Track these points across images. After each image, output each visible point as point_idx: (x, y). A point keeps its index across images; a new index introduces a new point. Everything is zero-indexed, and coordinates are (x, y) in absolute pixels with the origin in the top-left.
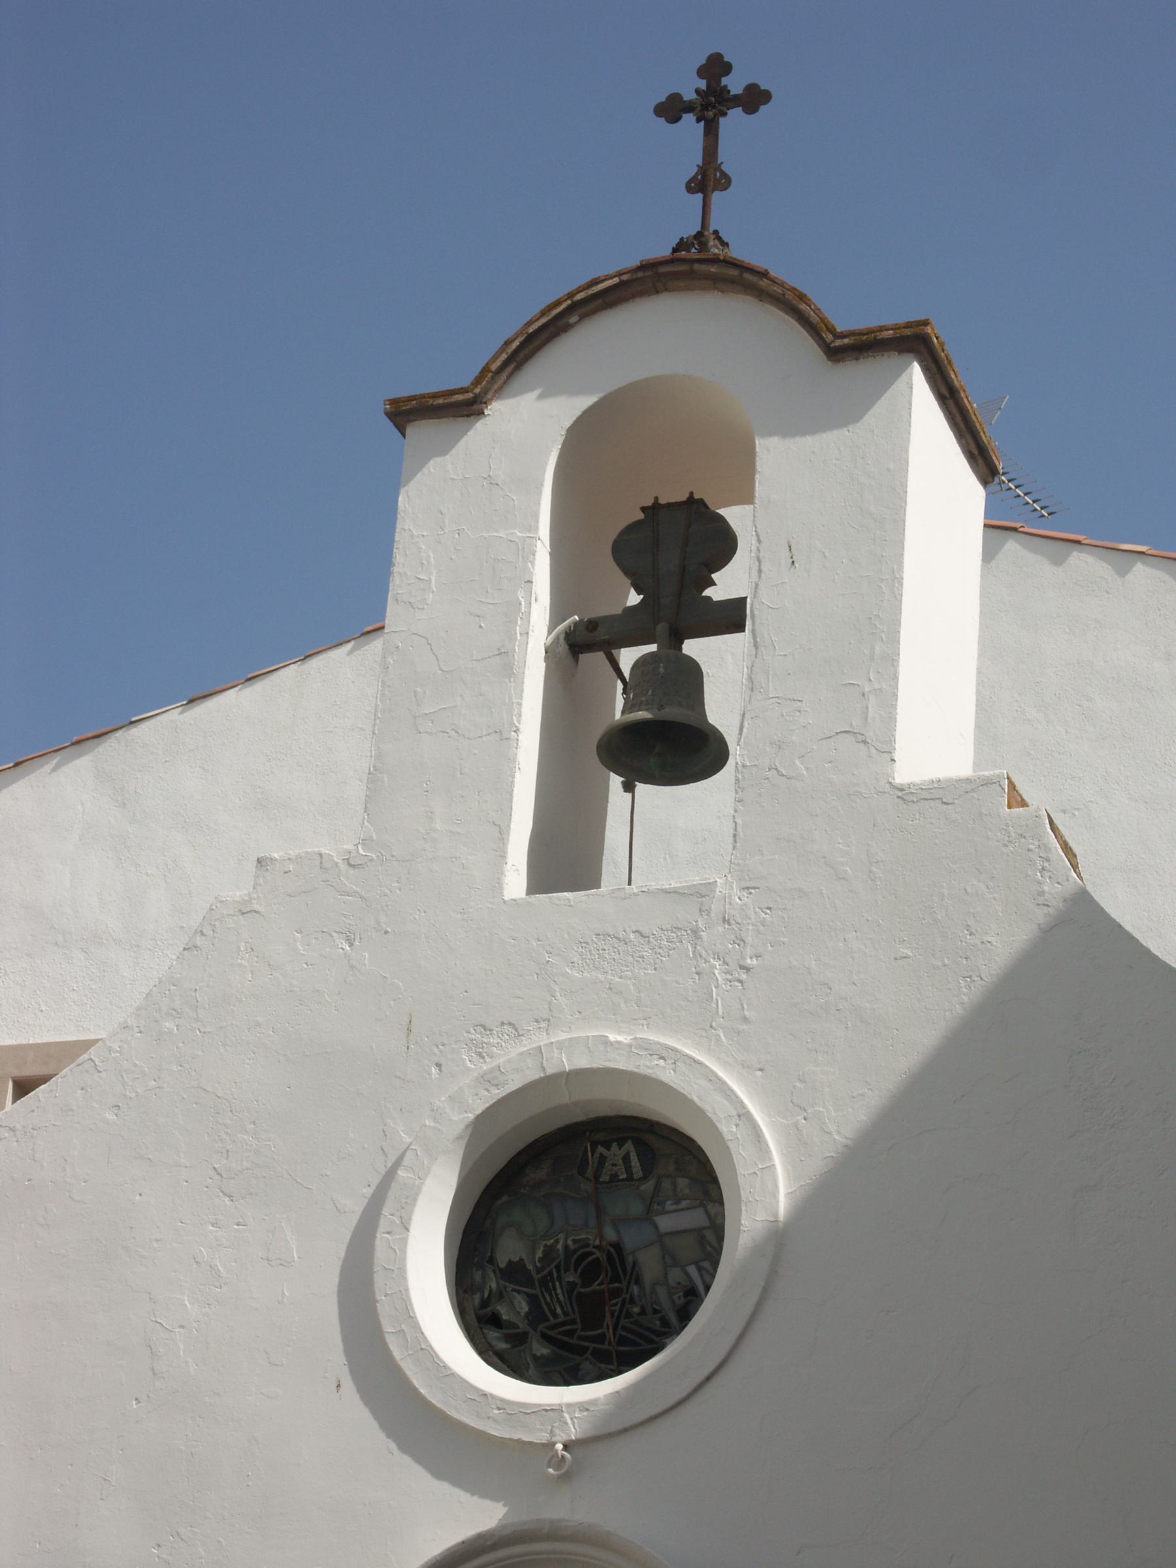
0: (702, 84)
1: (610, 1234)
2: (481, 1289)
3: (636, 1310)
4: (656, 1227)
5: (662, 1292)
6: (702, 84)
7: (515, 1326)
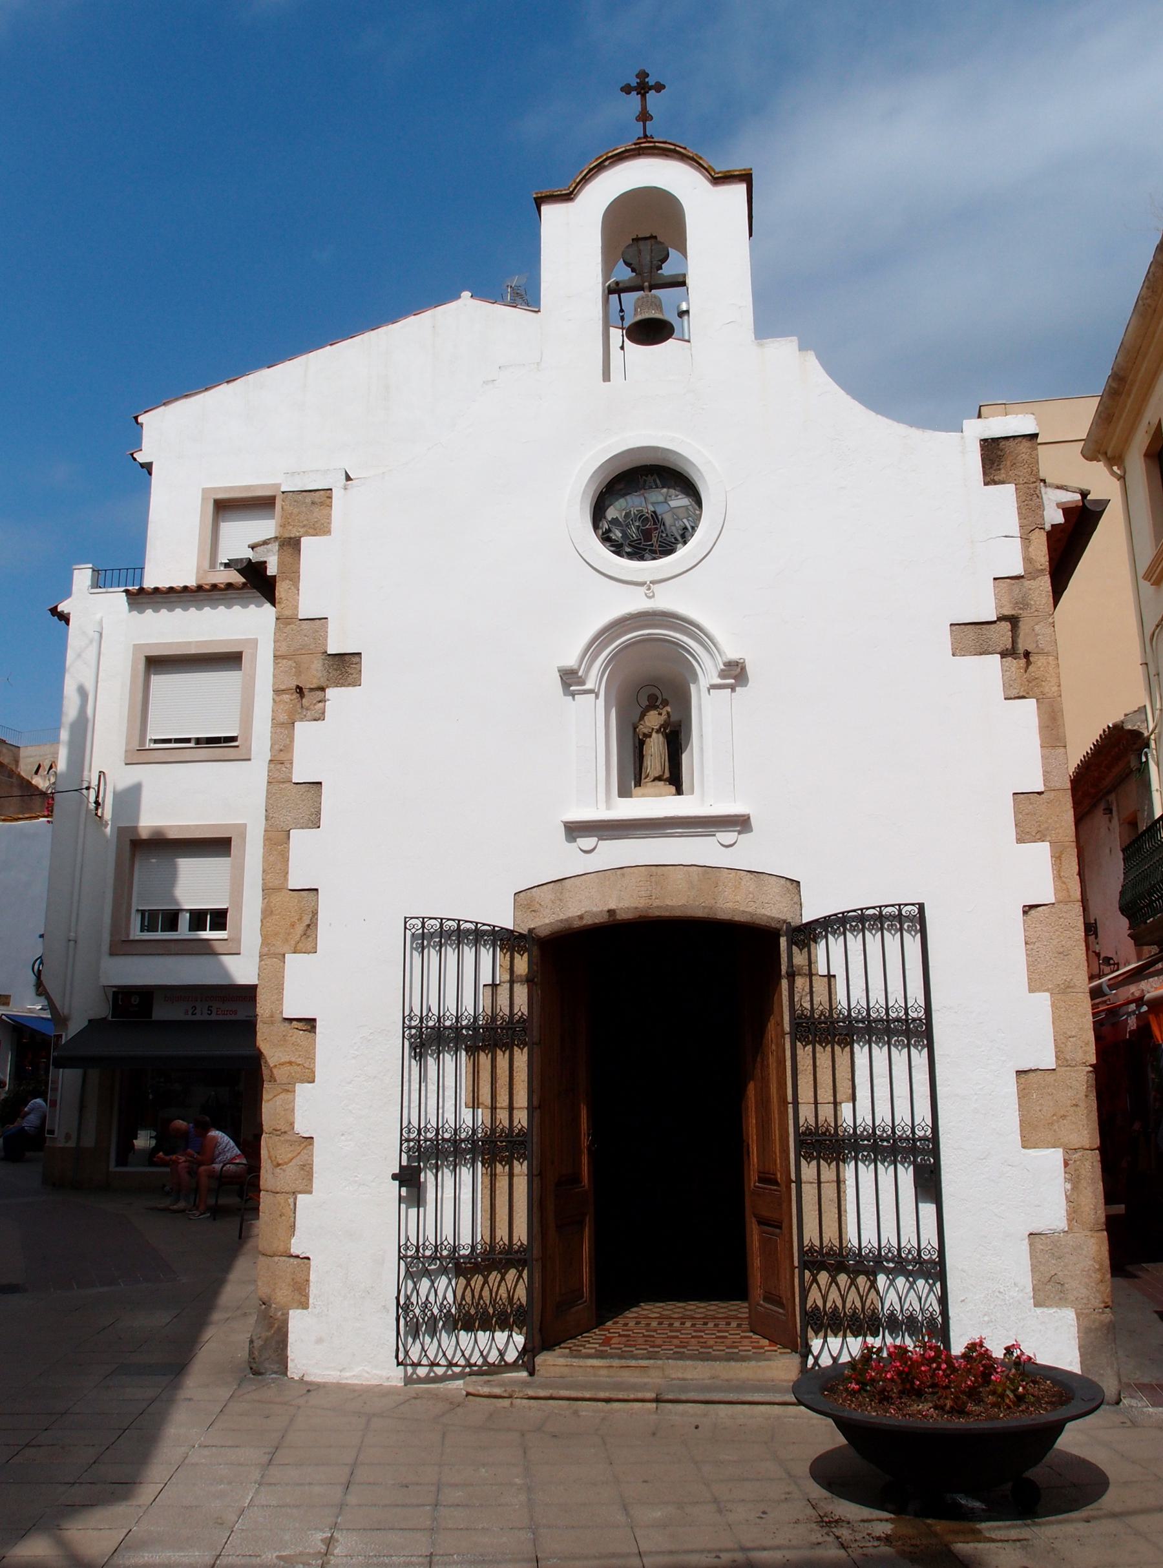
1: (651, 508)
2: (602, 528)
3: (664, 535)
5: (673, 528)
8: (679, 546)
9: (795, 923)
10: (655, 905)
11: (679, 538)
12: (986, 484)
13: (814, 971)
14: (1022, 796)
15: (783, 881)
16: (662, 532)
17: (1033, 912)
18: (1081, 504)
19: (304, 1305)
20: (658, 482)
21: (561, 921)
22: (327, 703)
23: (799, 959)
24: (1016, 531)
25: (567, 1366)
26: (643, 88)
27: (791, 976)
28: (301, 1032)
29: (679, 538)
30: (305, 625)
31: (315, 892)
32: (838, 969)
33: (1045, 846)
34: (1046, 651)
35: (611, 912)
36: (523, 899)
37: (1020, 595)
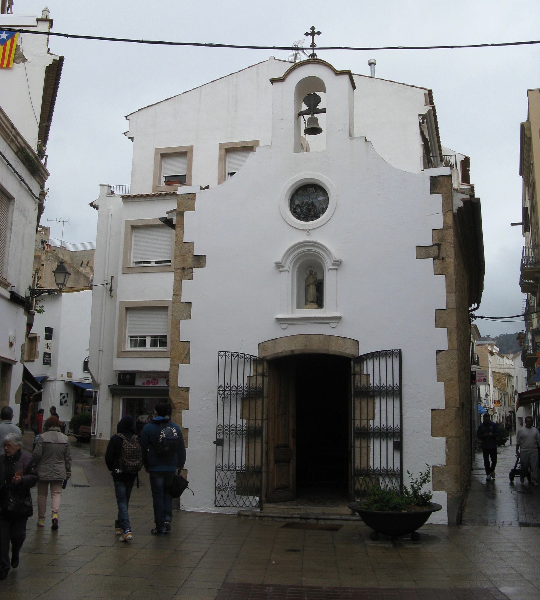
0: (311, 31)
1: (311, 200)
3: (316, 211)
4: (318, 199)
5: (319, 208)
6: (311, 31)
7: (299, 213)
8: (321, 215)
9: (356, 356)
10: (307, 349)
11: (321, 212)
12: (431, 194)
13: (362, 373)
14: (439, 311)
15: (353, 341)
16: (315, 209)
18: (470, 199)
23: (357, 369)
24: (441, 212)
25: (273, 508)
26: (313, 34)
27: (355, 374)
28: (184, 392)
29: (321, 212)
30: (186, 245)
32: (370, 372)
33: (446, 328)
35: (292, 351)
36: (262, 346)
37: (442, 236)
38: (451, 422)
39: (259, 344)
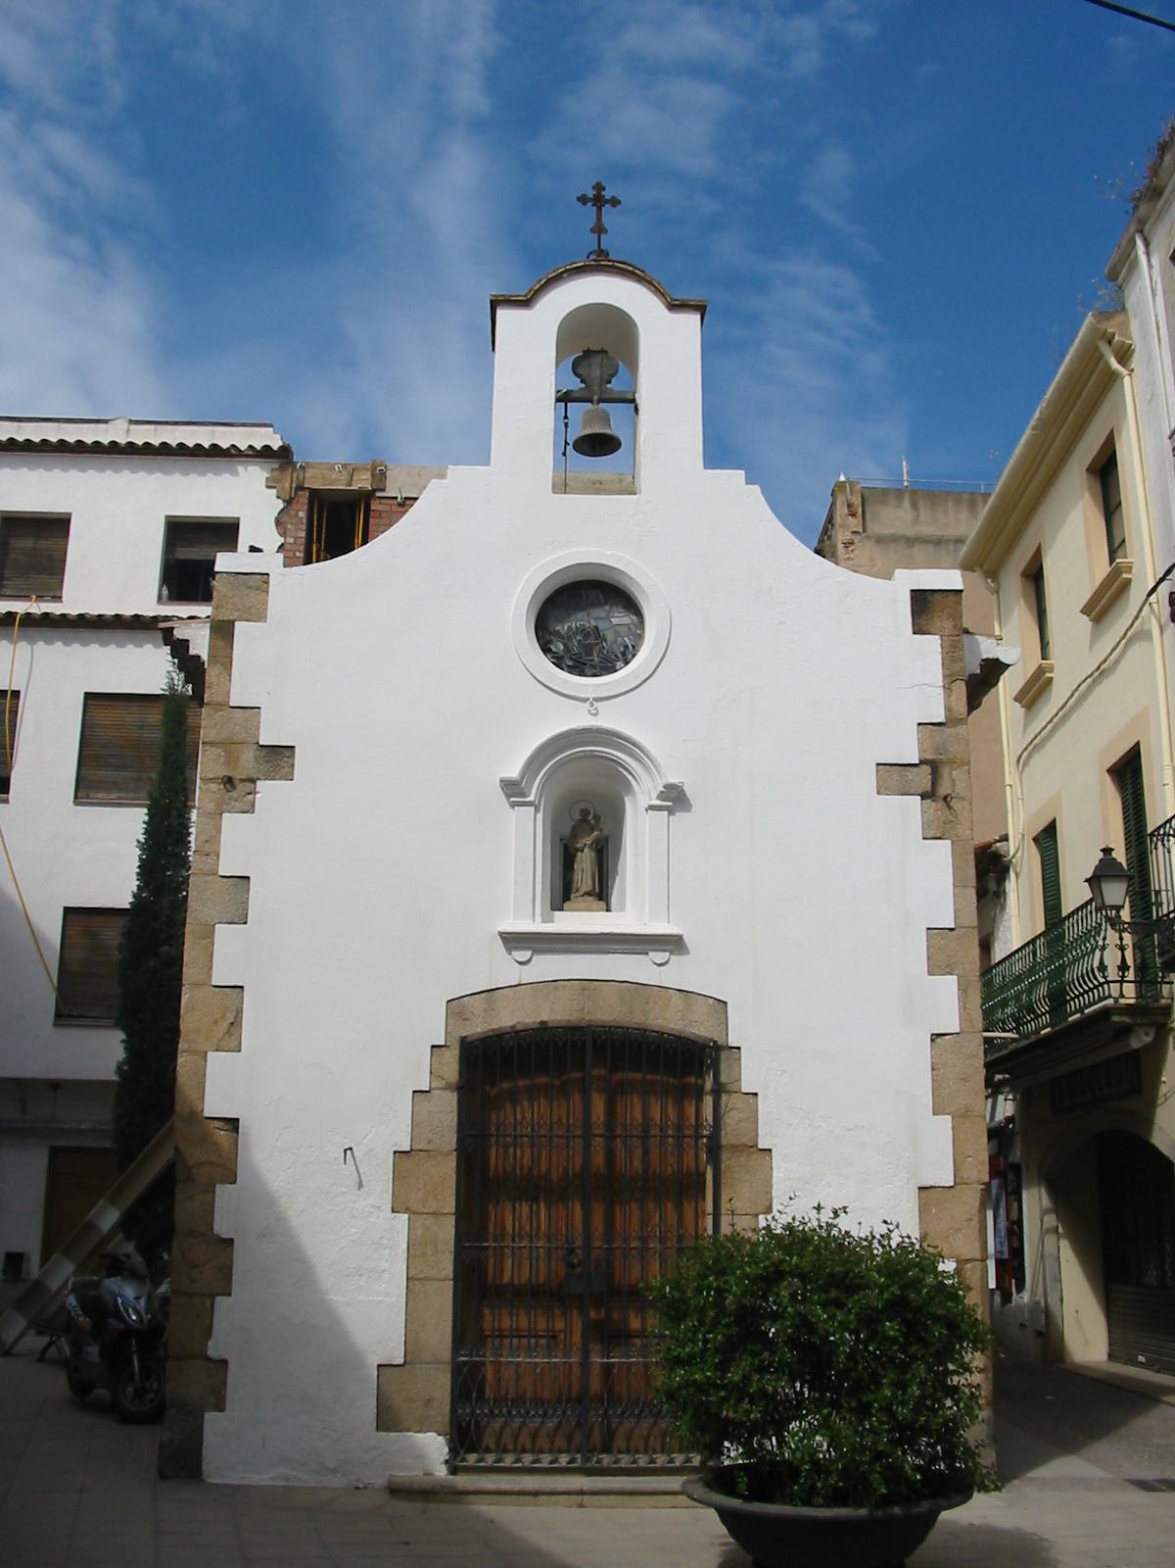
1: (593, 623)
11: (619, 655)
17: (939, 1040)
19: (220, 1407)
20: (601, 597)
21: (493, 1030)
22: (258, 796)
29: (619, 655)
31: (240, 990)
34: (962, 795)
38: (970, 1220)
39: (448, 1002)
